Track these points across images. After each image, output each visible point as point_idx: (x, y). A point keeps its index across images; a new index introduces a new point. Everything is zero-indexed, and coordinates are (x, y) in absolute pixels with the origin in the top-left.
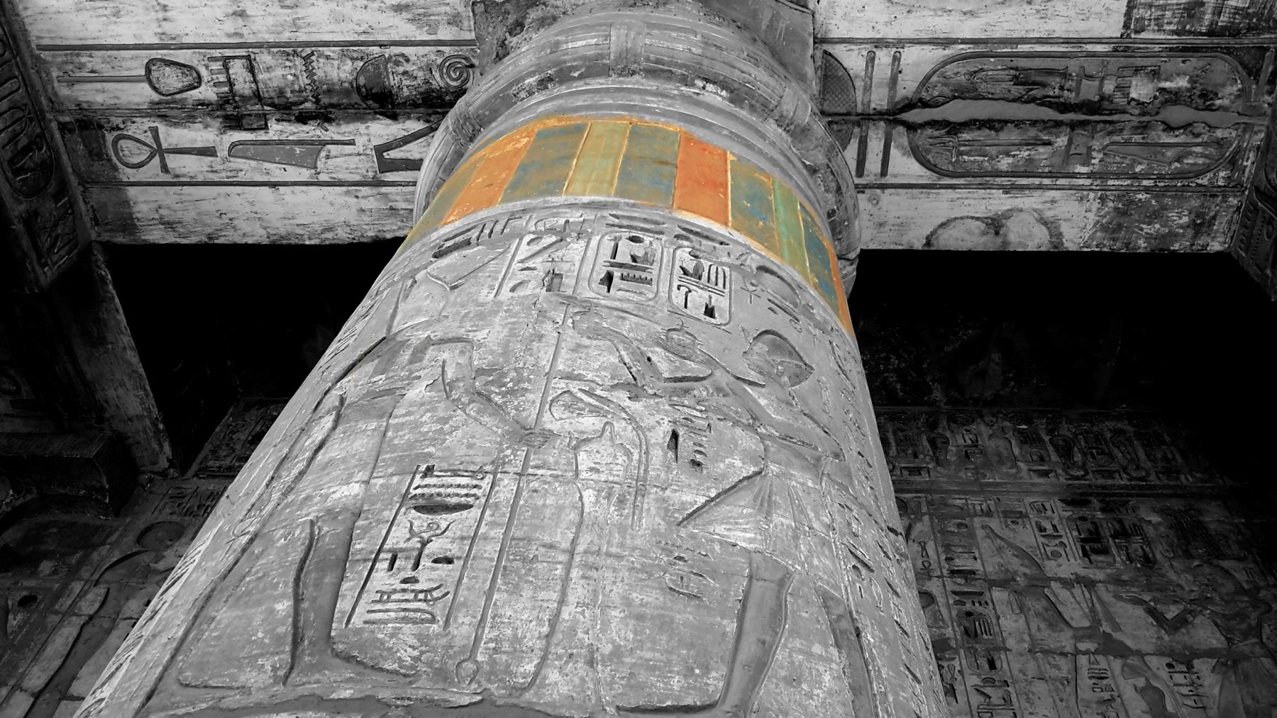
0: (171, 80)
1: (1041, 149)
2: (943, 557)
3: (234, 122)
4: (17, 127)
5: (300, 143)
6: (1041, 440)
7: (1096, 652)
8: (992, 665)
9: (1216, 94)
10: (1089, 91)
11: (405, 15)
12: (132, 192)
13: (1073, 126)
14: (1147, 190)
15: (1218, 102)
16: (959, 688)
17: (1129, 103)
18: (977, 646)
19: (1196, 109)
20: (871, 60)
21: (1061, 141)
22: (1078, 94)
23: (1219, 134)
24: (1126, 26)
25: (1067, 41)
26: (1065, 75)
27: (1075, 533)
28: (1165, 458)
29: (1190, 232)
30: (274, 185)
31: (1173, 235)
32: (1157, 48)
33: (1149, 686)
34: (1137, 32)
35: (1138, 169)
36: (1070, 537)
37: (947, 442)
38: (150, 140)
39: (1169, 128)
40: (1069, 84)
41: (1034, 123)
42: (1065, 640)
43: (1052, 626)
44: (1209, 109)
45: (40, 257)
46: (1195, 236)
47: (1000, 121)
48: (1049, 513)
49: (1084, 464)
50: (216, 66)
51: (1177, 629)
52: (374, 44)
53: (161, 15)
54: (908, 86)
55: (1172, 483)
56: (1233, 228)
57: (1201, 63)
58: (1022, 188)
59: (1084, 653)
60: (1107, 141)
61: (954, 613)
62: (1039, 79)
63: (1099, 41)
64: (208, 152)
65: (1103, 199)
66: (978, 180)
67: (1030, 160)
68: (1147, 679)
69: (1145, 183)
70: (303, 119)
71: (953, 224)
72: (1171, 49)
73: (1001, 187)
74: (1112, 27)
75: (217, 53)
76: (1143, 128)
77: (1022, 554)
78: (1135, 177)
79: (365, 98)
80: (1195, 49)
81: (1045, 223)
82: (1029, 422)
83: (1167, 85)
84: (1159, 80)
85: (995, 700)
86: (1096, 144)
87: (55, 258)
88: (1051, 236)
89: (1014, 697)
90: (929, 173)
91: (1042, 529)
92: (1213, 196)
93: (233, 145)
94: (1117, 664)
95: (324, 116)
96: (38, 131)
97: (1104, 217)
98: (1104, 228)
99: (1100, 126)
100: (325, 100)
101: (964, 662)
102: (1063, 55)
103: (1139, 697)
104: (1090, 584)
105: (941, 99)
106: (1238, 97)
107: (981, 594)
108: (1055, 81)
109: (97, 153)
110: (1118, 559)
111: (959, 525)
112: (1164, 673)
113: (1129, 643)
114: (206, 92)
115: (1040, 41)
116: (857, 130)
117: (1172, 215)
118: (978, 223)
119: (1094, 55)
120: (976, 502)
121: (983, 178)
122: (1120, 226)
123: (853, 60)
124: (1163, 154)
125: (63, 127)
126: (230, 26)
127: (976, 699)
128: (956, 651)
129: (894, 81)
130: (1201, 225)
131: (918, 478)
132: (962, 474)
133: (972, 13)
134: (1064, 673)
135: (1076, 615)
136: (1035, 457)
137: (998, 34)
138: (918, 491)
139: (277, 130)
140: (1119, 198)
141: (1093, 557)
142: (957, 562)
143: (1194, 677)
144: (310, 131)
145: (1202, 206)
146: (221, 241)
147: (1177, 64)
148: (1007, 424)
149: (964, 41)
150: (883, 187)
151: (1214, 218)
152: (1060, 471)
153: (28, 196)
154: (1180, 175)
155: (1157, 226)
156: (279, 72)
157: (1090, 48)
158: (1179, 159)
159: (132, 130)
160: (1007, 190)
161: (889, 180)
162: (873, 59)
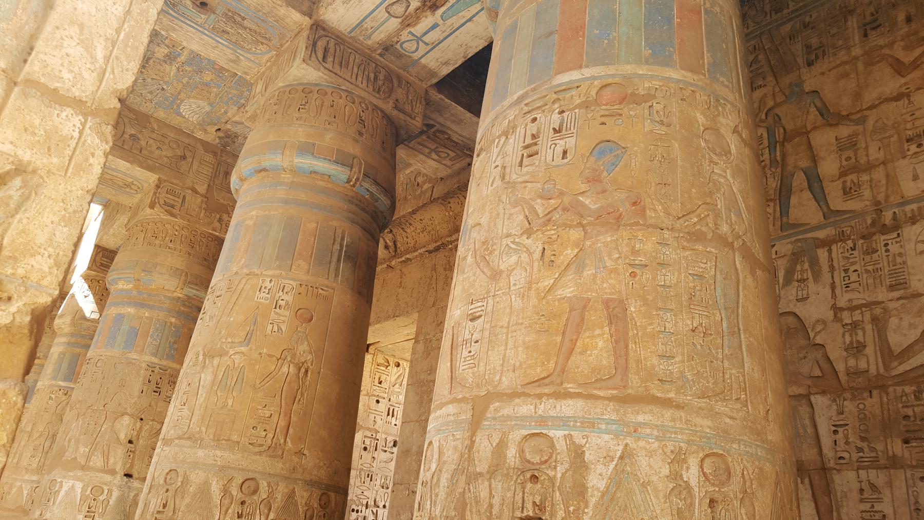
4: (366, 73)
12: (423, 61)
30: (470, 20)
38: (413, 38)
64: (435, 26)
93: (442, 17)
109: (400, 56)
153: (389, 97)
159: (403, 38)
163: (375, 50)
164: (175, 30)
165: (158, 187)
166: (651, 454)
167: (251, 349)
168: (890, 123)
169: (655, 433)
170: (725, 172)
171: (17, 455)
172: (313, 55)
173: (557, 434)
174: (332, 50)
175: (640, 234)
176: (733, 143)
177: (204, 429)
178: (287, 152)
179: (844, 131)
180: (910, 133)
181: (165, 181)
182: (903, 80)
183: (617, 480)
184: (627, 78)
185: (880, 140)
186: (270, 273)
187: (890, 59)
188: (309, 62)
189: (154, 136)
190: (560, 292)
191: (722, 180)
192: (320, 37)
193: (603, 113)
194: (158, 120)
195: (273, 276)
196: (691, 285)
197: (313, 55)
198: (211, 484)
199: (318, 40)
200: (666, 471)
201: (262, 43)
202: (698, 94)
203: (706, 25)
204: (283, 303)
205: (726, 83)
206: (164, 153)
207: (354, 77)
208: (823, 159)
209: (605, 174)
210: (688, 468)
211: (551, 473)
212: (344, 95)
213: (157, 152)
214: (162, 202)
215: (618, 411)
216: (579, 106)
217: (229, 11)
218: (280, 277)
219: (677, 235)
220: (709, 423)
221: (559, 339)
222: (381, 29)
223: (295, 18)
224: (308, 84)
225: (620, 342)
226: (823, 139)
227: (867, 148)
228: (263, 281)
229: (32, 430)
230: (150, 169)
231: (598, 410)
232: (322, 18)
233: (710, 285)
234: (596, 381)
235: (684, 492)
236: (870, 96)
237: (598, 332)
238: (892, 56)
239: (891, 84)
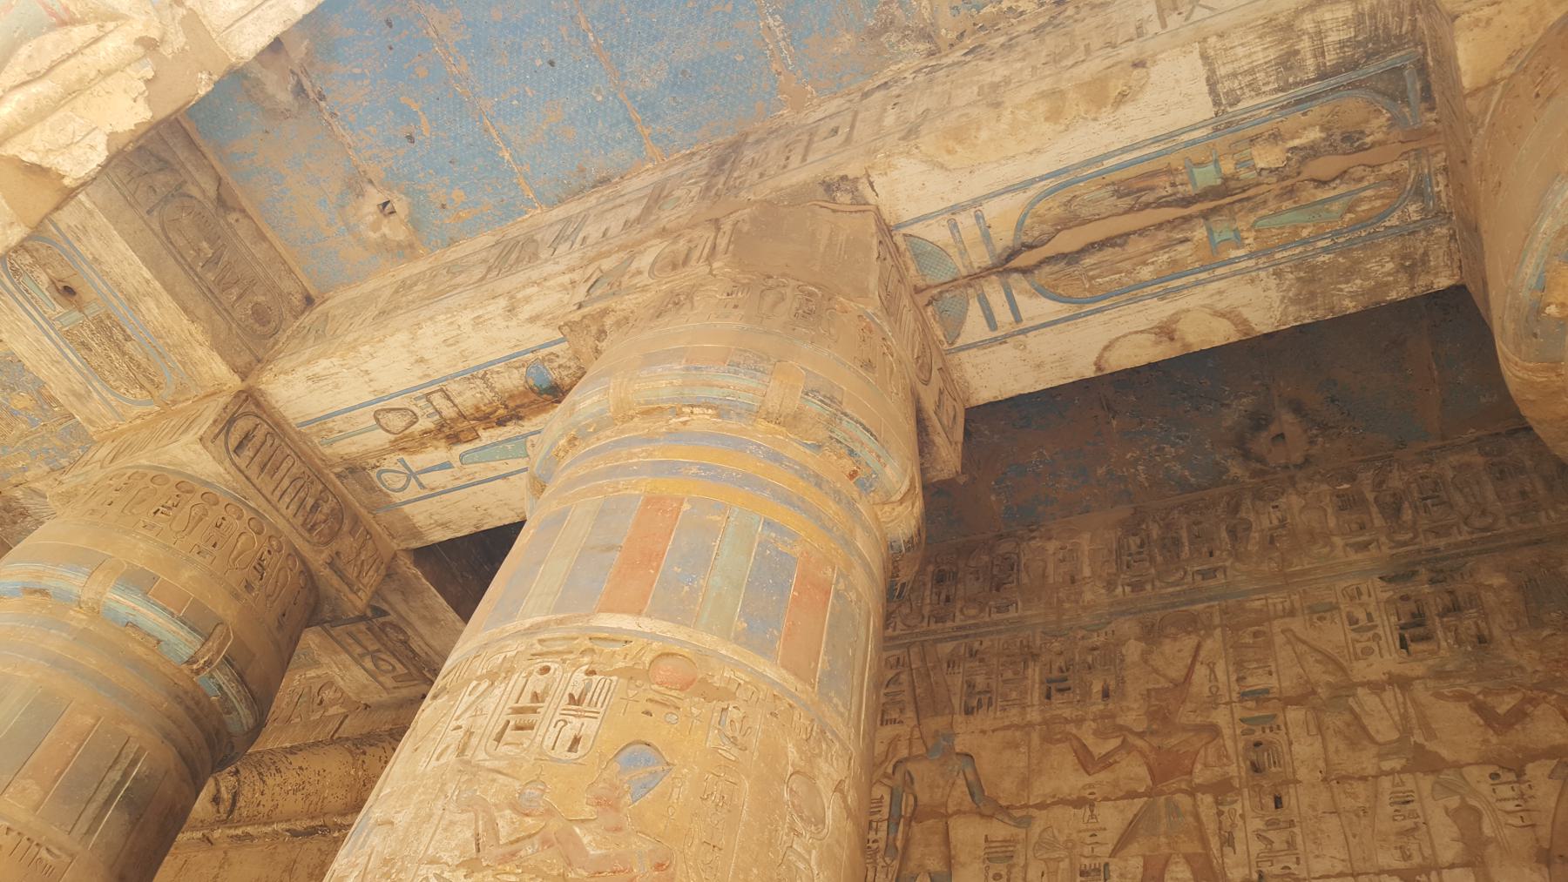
0: (397, 422)
1: (1180, 248)
2: (1234, 678)
3: (454, 439)
4: (302, 494)
5: (509, 440)
6: (1364, 501)
7: (1404, 770)
8: (1278, 802)
9: (1362, 132)
10: (1206, 177)
11: (540, 323)
12: (407, 508)
13: (1205, 216)
14: (1326, 250)
15: (1368, 140)
16: (1239, 835)
17: (1259, 174)
18: (1264, 782)
19: (1345, 154)
20: (954, 226)
21: (1200, 233)
22: (1195, 185)
23: (1387, 170)
24: (1216, 103)
25: (1156, 140)
26: (1170, 171)
27: (1394, 619)
28: (1523, 494)
29: (1403, 277)
30: (504, 477)
31: (1383, 286)
32: (1264, 112)
33: (1464, 806)
34: (1231, 105)
35: (1305, 233)
36: (1387, 625)
37: (1249, 529)
38: (402, 469)
39: (1321, 183)
40: (1178, 179)
41: (1159, 226)
42: (1367, 761)
43: (1353, 744)
44: (1361, 149)
45: (350, 586)
46: (1412, 277)
47: (1120, 236)
48: (1365, 598)
49: (1415, 523)
50: (422, 403)
51: (1511, 726)
52: (526, 352)
53: (367, 378)
54: (1004, 237)
55: (1525, 526)
56: (1456, 257)
57: (1326, 109)
58: (1178, 290)
59: (1387, 774)
60: (1252, 218)
61: (1241, 745)
62: (1142, 185)
63: (1193, 128)
64: (446, 466)
65: (1278, 274)
66: (1124, 297)
67: (1173, 262)
68: (1463, 799)
69: (1321, 244)
70: (501, 422)
71: (1117, 345)
72: (1283, 107)
73: (1154, 295)
74: (1203, 109)
75: (418, 393)
76: (1290, 192)
77: (1327, 658)
78: (1305, 242)
79: (540, 394)
80: (1313, 97)
81: (1223, 315)
82: (1352, 478)
83: (1296, 142)
84: (1284, 141)
85: (1277, 846)
86: (1241, 224)
87: (365, 581)
88: (1236, 325)
89: (1299, 839)
90: (1066, 306)
91: (1353, 621)
92: (1413, 233)
93: (461, 456)
94: (1426, 782)
95: (515, 416)
96: (321, 487)
97: (1289, 290)
98: (1295, 301)
99: (1237, 206)
100: (511, 404)
101: (1247, 803)
102: (1159, 154)
103: (1450, 821)
104: (1403, 683)
105: (1045, 237)
106: (1391, 126)
107: (1274, 716)
108: (1162, 181)
109: (371, 488)
110: (1444, 644)
111: (1255, 635)
112: (1485, 788)
113: (1445, 753)
114: (425, 423)
115: (1124, 150)
116: (970, 291)
117: (1372, 265)
118: (1145, 336)
119: (1194, 142)
120: (1277, 600)
121: (1131, 292)
122: (1313, 295)
123: (937, 233)
124: (1328, 211)
125: (338, 476)
126: (418, 371)
127: (1257, 847)
128: (1239, 792)
129: (987, 238)
130: (1412, 266)
131: (1212, 583)
132: (1264, 567)
133: (1038, 151)
134: (1361, 802)
135: (1383, 728)
136: (1354, 526)
137: (1076, 159)
138: (1210, 599)
139: (487, 436)
140: (1297, 268)
141: (1413, 647)
142: (1251, 681)
143: (1524, 787)
144: (511, 430)
145: (1404, 247)
146: (486, 527)
147: (1295, 119)
148: (1324, 487)
149: (1042, 178)
150: (1024, 332)
151: (1425, 254)
152: (1383, 539)
153: (326, 543)
154: (1361, 223)
155: (1358, 282)
156: (469, 394)
157: (1185, 137)
158: (1350, 210)
159: (386, 465)
160: (1162, 296)
161: (1026, 324)
162: (955, 225)
163: (332, 466)
168: (1062, 839)
170: (810, 853)
172: (222, 436)
174: (257, 441)
176: (832, 809)
179: (1000, 830)
180: (1086, 862)
182: (1088, 780)
185: (1045, 861)
187: (1075, 743)
191: (802, 866)
192: (245, 414)
197: (222, 436)
201: (142, 387)
205: (842, 709)
207: (278, 493)
208: (963, 865)
212: (247, 515)
216: (619, 672)
217: (109, 317)
222: (355, 438)
223: (217, 371)
224: (190, 477)
226: (968, 833)
227: (1026, 866)
236: (1042, 788)
238: (1079, 740)
239: (1072, 781)
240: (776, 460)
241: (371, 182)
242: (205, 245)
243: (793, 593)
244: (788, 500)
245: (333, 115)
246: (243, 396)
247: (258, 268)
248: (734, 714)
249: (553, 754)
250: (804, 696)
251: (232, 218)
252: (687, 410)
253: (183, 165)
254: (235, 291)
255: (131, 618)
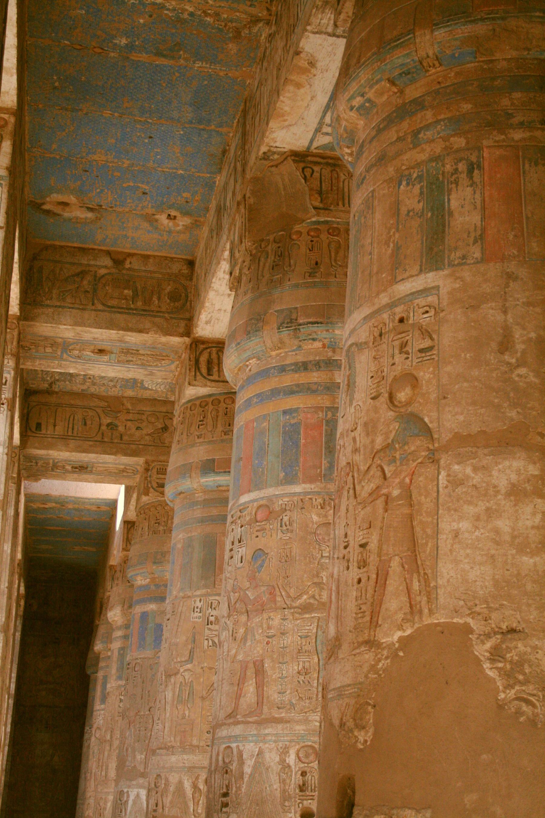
164: (89, 369)
165: (147, 470)
166: (271, 750)
167: (195, 665)
169: (273, 738)
171: (104, 767)
172: (198, 374)
173: (234, 745)
175: (272, 614)
177: (172, 739)
178: (193, 475)
181: (153, 461)
183: (255, 768)
184: (270, 499)
186: (198, 593)
188: (195, 382)
189: (131, 417)
190: (238, 658)
192: (201, 353)
193: (258, 528)
194: (131, 398)
195: (201, 595)
196: (299, 643)
197: (198, 374)
198: (183, 783)
199: (199, 357)
200: (277, 759)
202: (314, 500)
203: (326, 436)
204: (212, 619)
206: (144, 432)
209: (257, 574)
210: (289, 756)
211: (231, 767)
213: (138, 433)
214: (155, 485)
215: (256, 729)
218: (207, 595)
219: (292, 611)
220: (304, 728)
221: (236, 688)
223: (176, 341)
225: (260, 686)
228: (195, 601)
229: (111, 737)
230: (134, 453)
231: (249, 730)
232: (197, 335)
233: (312, 640)
234: (251, 712)
235: (287, 769)
237: (251, 682)
240: (282, 371)
241: (154, 215)
242: (126, 291)
243: (303, 441)
244: (291, 391)
245: (112, 207)
246: (194, 346)
247: (157, 275)
248: (286, 519)
249: (238, 566)
250: (316, 490)
251: (127, 265)
252: (248, 363)
253: (89, 265)
254: (155, 299)
255: (216, 485)
